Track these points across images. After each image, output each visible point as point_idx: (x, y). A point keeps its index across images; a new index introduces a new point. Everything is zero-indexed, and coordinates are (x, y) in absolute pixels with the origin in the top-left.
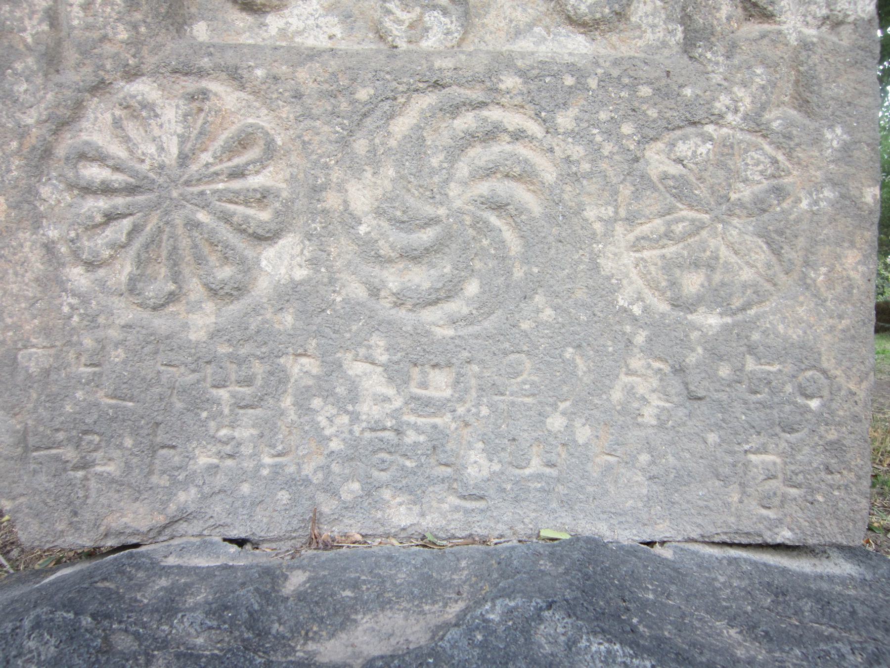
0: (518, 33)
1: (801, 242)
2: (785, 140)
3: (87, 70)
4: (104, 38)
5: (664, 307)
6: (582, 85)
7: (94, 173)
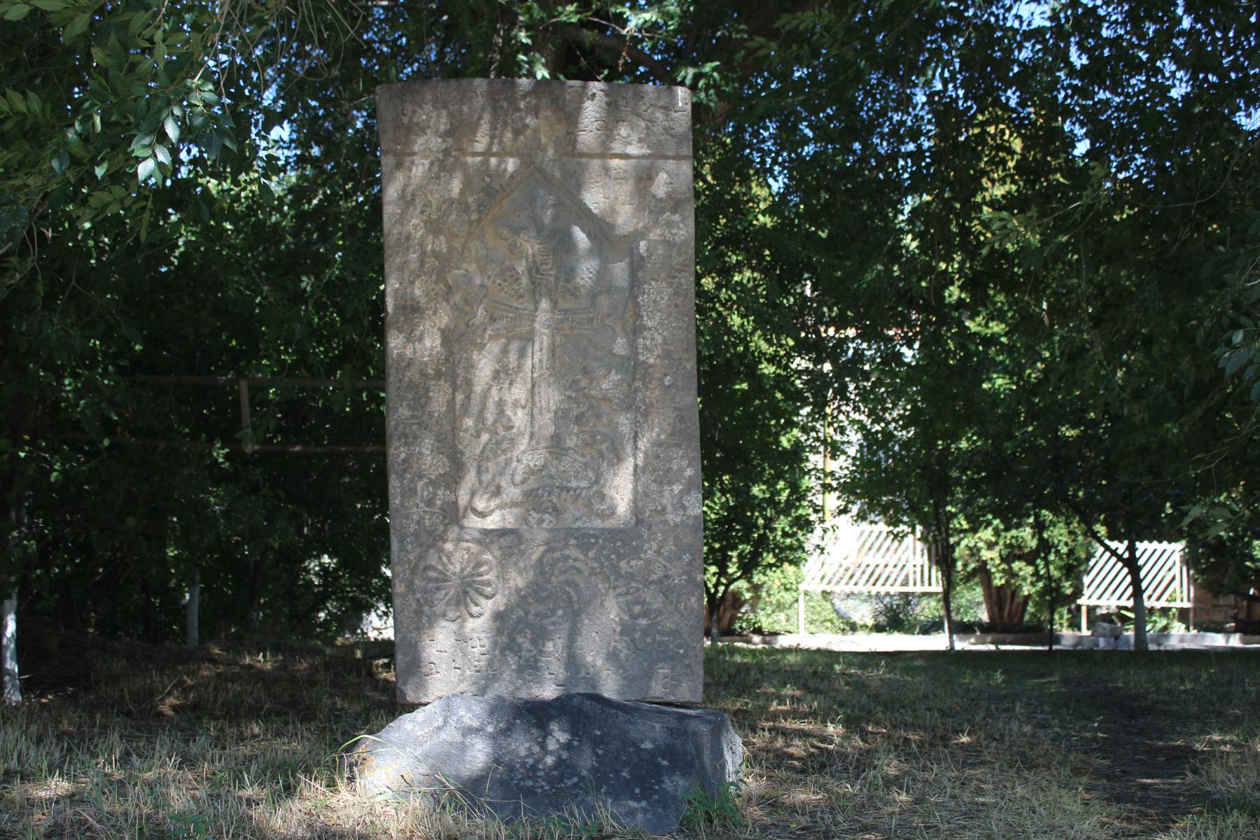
0: (577, 520)
1: (675, 594)
2: (669, 559)
5: (627, 618)
6: (597, 542)
7: (432, 574)
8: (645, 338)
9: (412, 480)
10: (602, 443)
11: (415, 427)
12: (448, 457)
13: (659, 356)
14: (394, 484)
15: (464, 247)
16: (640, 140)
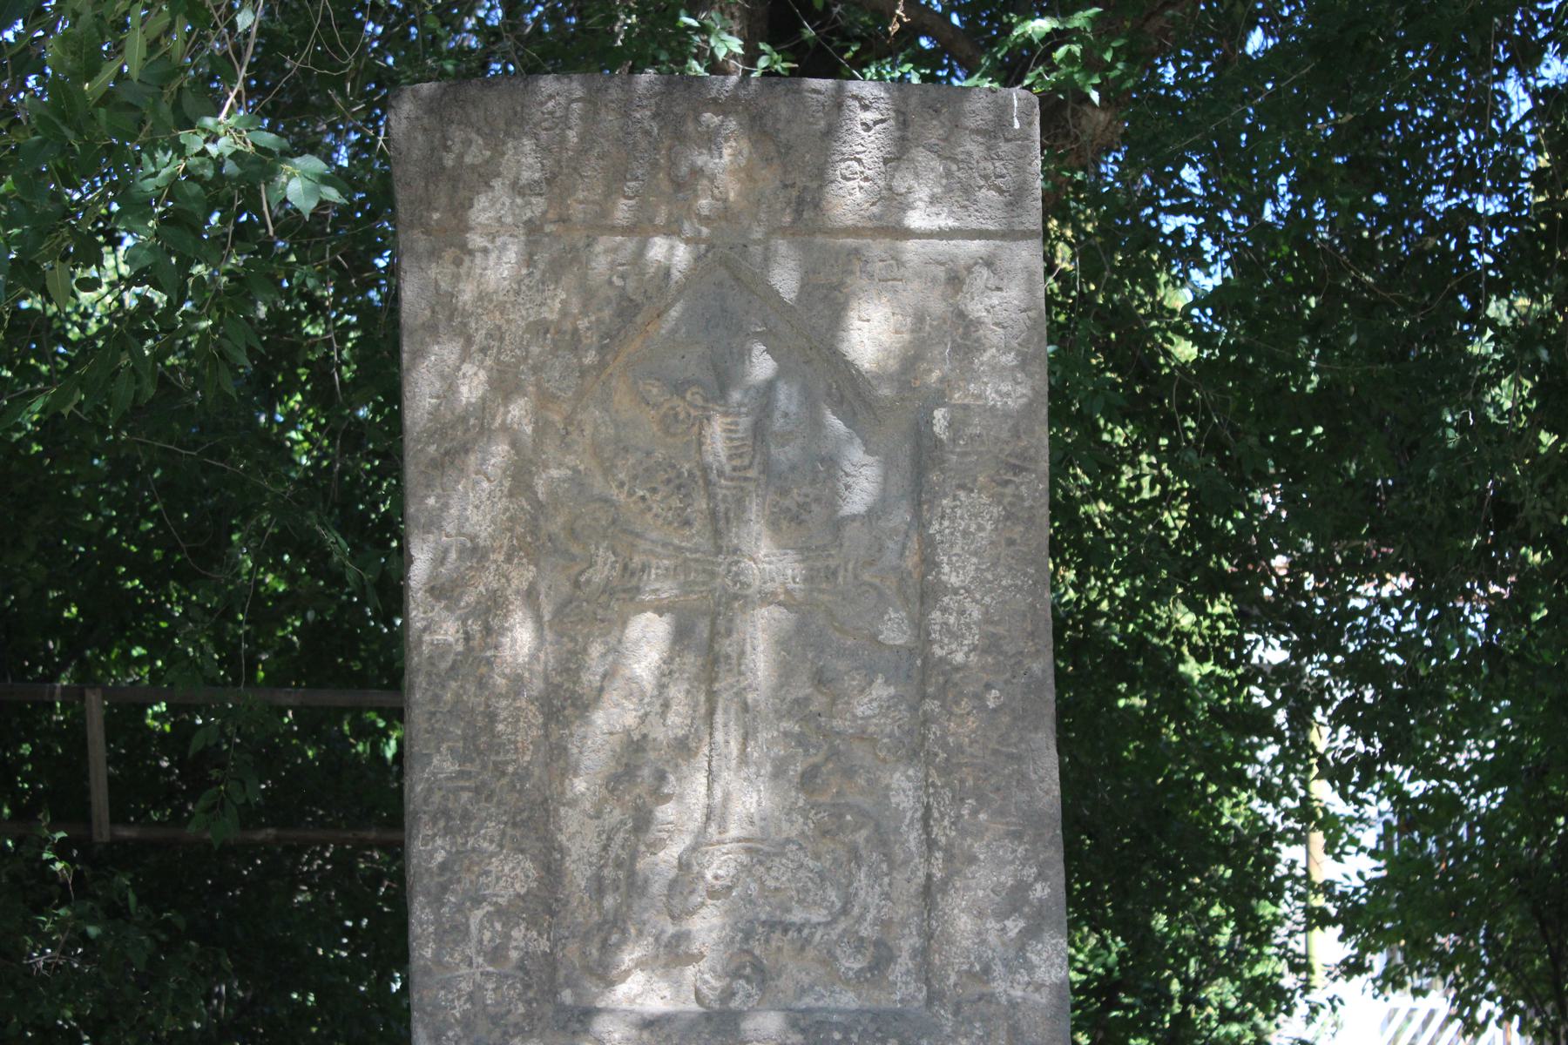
0: (802, 992)
3: (497, 1034)
4: (509, 1011)
8: (944, 610)
9: (459, 908)
10: (858, 827)
11: (465, 796)
12: (534, 859)
13: (974, 648)
14: (422, 917)
15: (569, 420)
16: (934, 200)
